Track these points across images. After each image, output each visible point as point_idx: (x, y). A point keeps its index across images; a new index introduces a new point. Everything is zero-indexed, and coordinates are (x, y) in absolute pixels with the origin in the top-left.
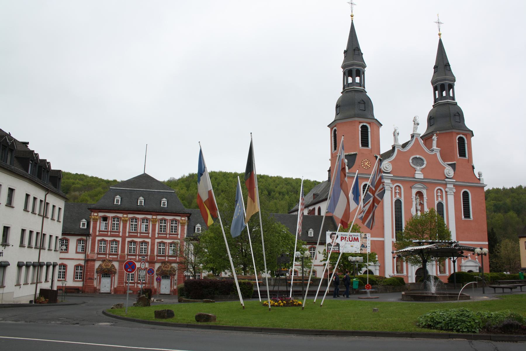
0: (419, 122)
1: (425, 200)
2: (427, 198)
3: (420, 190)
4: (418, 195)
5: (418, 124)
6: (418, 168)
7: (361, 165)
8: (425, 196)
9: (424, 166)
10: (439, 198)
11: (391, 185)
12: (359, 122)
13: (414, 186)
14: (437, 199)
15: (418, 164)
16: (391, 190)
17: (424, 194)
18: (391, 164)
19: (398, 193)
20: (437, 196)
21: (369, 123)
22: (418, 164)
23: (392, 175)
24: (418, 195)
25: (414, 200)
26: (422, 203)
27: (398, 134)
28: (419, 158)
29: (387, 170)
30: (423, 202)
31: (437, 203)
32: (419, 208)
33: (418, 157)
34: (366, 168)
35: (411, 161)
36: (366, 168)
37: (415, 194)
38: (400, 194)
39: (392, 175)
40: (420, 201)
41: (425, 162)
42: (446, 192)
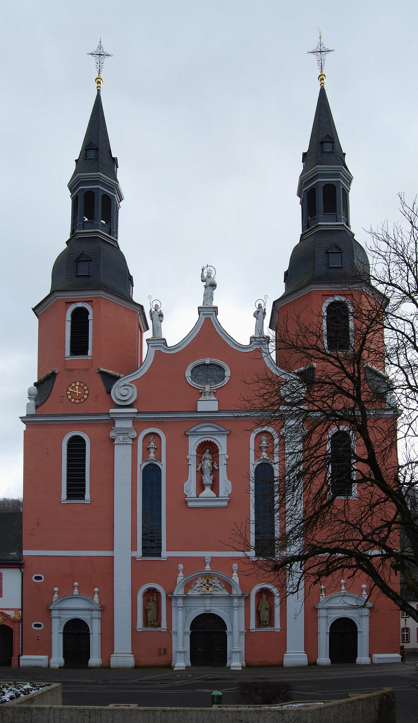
0: (217, 281)
1: (222, 461)
2: (227, 457)
3: (209, 439)
4: (208, 450)
5: (213, 286)
6: (207, 388)
7: (65, 395)
8: (223, 451)
9: (227, 380)
10: (264, 454)
11: (134, 434)
12: (66, 303)
13: (192, 430)
14: (257, 457)
15: (209, 380)
16: (132, 445)
17: (219, 448)
18: (134, 386)
19: (152, 450)
20: (258, 450)
21: (89, 302)
22: (211, 378)
23: (135, 410)
24: (208, 450)
25: (193, 461)
26: (216, 468)
27: (161, 315)
28: (211, 364)
29: (125, 401)
30: (218, 466)
31: (255, 466)
32: (208, 479)
33: (208, 361)
34: (77, 401)
35: (188, 374)
36: (77, 401)
37: (196, 448)
38: (158, 450)
39: (135, 410)
40: (212, 464)
41: (228, 373)
42: (282, 437)
